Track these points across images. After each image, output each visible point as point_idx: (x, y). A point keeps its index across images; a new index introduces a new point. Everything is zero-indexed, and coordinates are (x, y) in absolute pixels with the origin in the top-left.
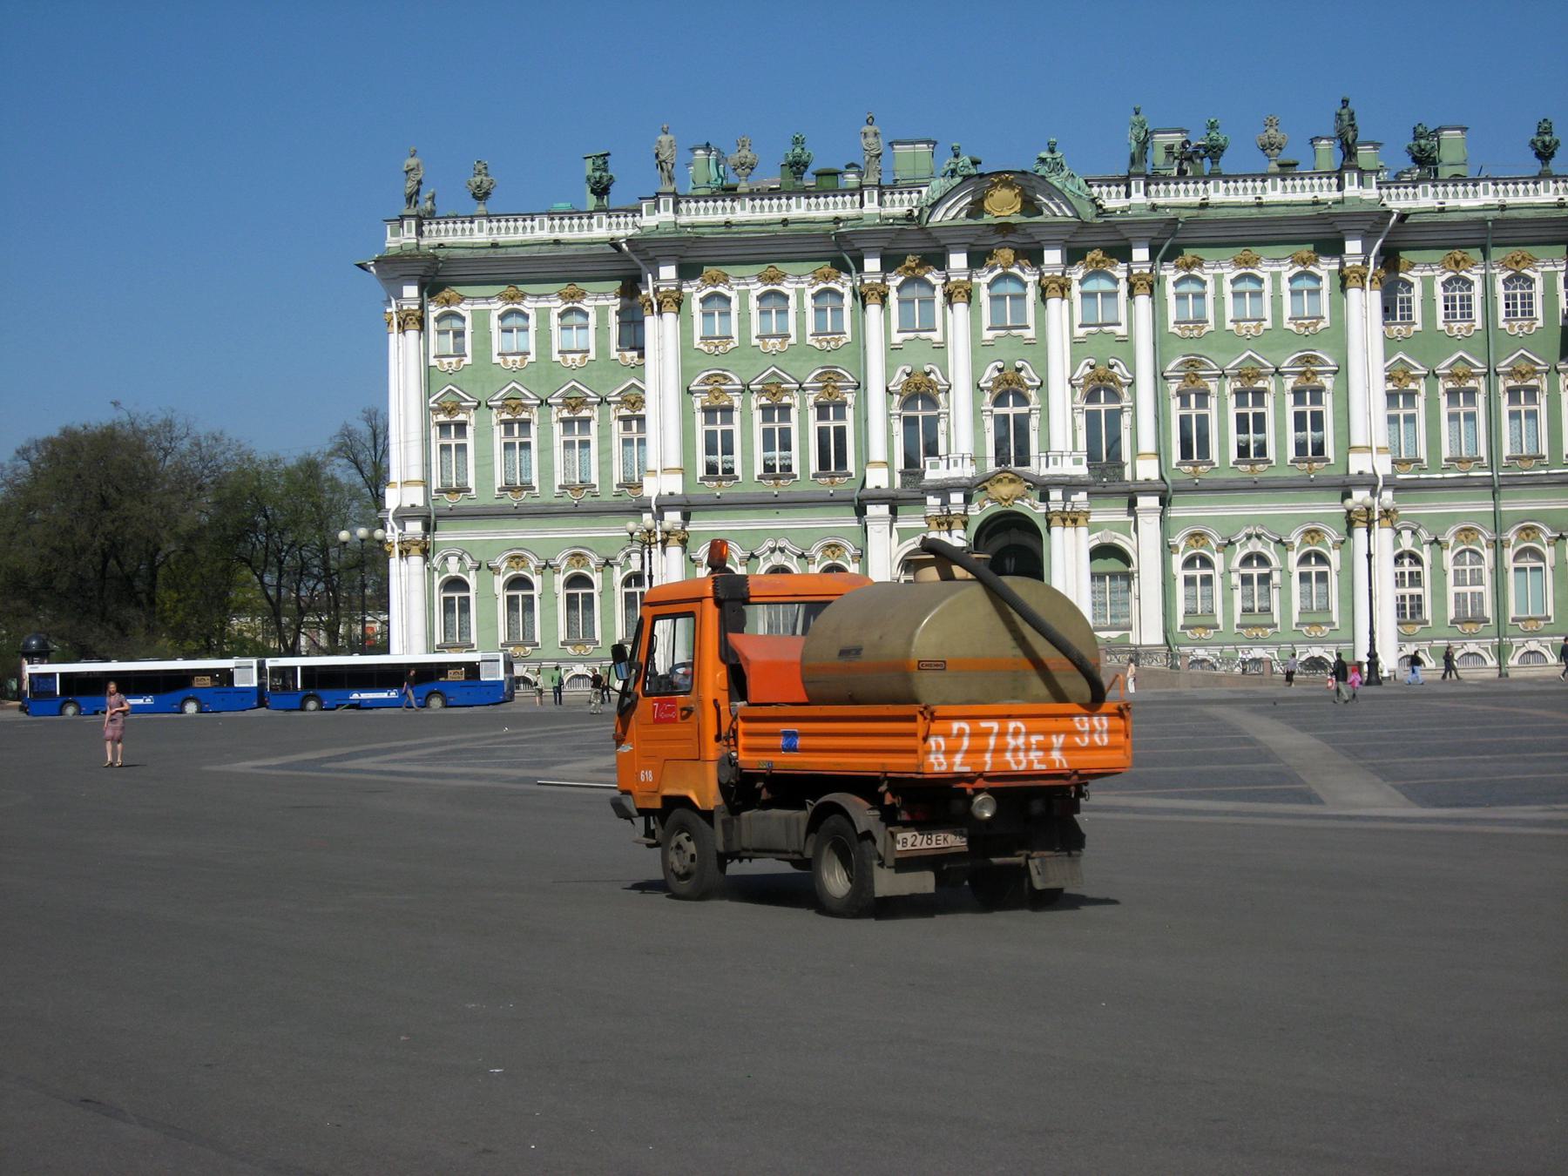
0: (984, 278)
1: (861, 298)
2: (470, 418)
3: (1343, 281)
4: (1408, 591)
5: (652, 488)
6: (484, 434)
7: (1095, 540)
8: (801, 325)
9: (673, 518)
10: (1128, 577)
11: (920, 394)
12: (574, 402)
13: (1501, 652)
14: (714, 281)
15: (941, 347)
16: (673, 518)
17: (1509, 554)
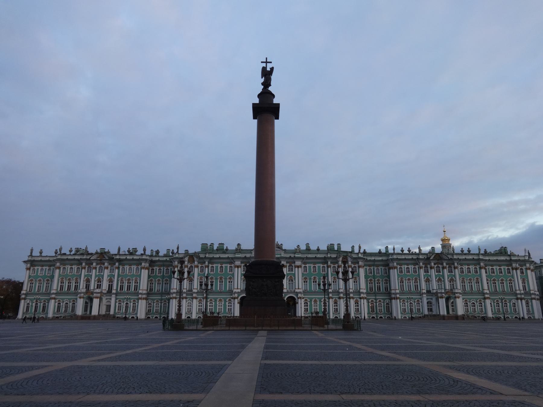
1: (82, 269)
3: (141, 268)
5: (53, 292)
11: (88, 281)
12: (48, 280)
13: (160, 316)
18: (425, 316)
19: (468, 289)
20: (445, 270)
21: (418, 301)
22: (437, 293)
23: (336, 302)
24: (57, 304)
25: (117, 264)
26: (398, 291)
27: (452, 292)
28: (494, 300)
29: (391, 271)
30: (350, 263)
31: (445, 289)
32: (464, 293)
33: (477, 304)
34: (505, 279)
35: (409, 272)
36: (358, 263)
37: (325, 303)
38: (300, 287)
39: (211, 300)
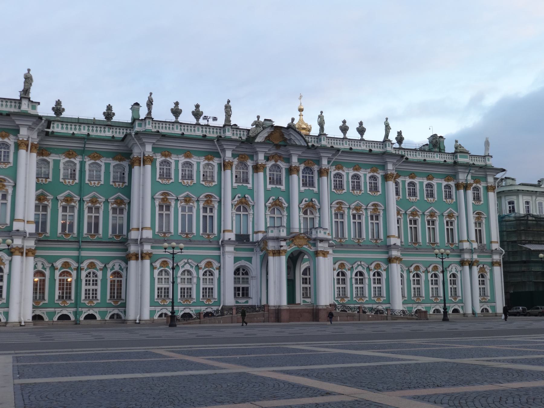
18: (226, 310)
19: (349, 233)
20: (295, 177)
21: (209, 264)
22: (265, 240)
26: (148, 234)
27: (309, 239)
28: (409, 265)
29: (136, 169)
31: (289, 232)
32: (340, 245)
33: (369, 276)
34: (438, 213)
35: (191, 177)
36: (17, 131)
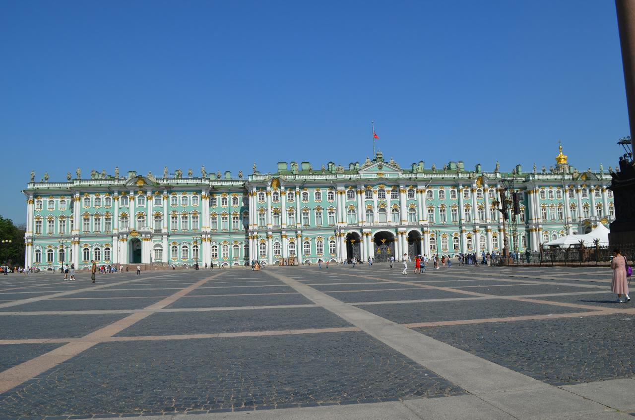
0: (137, 197)
1: (114, 199)
2: (42, 220)
4: (215, 252)
5: (74, 233)
6: (45, 223)
7: (156, 243)
8: (103, 204)
9: (77, 239)
10: (162, 250)
14: (87, 196)
15: (128, 208)
16: (77, 239)
17: (233, 246)
23: (469, 238)
24: (82, 249)
25: (165, 193)
30: (486, 186)
36: (496, 185)
37: (455, 238)
38: (425, 219)
39: (307, 238)
